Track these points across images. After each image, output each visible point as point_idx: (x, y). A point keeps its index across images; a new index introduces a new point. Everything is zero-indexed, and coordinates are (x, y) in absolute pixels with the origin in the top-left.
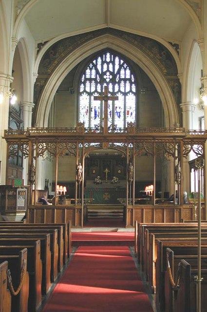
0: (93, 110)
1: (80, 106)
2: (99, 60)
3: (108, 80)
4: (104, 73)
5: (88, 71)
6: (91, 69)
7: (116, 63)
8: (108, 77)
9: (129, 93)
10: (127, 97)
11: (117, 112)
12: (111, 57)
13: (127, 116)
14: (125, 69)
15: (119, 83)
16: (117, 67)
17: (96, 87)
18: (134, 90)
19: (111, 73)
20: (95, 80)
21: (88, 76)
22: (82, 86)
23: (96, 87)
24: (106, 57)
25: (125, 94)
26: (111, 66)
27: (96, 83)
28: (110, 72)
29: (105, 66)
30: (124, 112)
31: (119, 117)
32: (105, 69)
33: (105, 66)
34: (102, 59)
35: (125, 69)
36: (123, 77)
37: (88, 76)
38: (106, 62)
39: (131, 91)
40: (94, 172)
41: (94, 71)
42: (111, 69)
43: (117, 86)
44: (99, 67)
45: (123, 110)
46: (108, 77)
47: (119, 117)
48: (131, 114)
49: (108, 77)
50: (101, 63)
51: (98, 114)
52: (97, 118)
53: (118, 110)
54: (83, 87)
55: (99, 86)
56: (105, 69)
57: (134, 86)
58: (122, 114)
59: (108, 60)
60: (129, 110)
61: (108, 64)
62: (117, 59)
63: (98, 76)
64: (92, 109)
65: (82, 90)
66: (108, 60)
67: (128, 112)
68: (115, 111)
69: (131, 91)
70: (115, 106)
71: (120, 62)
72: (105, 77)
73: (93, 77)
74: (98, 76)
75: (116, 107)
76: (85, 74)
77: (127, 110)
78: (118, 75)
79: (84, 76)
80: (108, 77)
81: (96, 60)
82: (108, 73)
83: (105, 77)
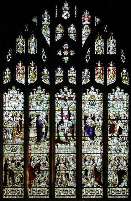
0: (33, 122)
1: (5, 113)
3: (66, 59)
5: (20, 41)
6: (27, 38)
8: (66, 54)
9: (113, 86)
10: (111, 97)
11: (87, 127)
15: (92, 68)
16: (86, 32)
17: (39, 75)
19: (74, 45)
20: (37, 57)
22: (8, 72)
23: (39, 75)
25: (105, 90)
26: (72, 29)
27: (40, 67)
31: (93, 136)
32: (59, 37)
36: (99, 51)
37: (20, 51)
38: (60, 20)
41: (33, 42)
43: (86, 73)
44: (46, 32)
47: (93, 136)
49: (66, 54)
51: (44, 130)
52: (43, 139)
56: (59, 37)
58: (98, 133)
59: (66, 15)
60: (114, 122)
62: (86, 16)
63: (43, 50)
64: (31, 119)
67: (113, 126)
73: (32, 51)
74: (43, 50)
75: (86, 117)
78: (89, 50)
79: (10, 50)
82: (66, 46)
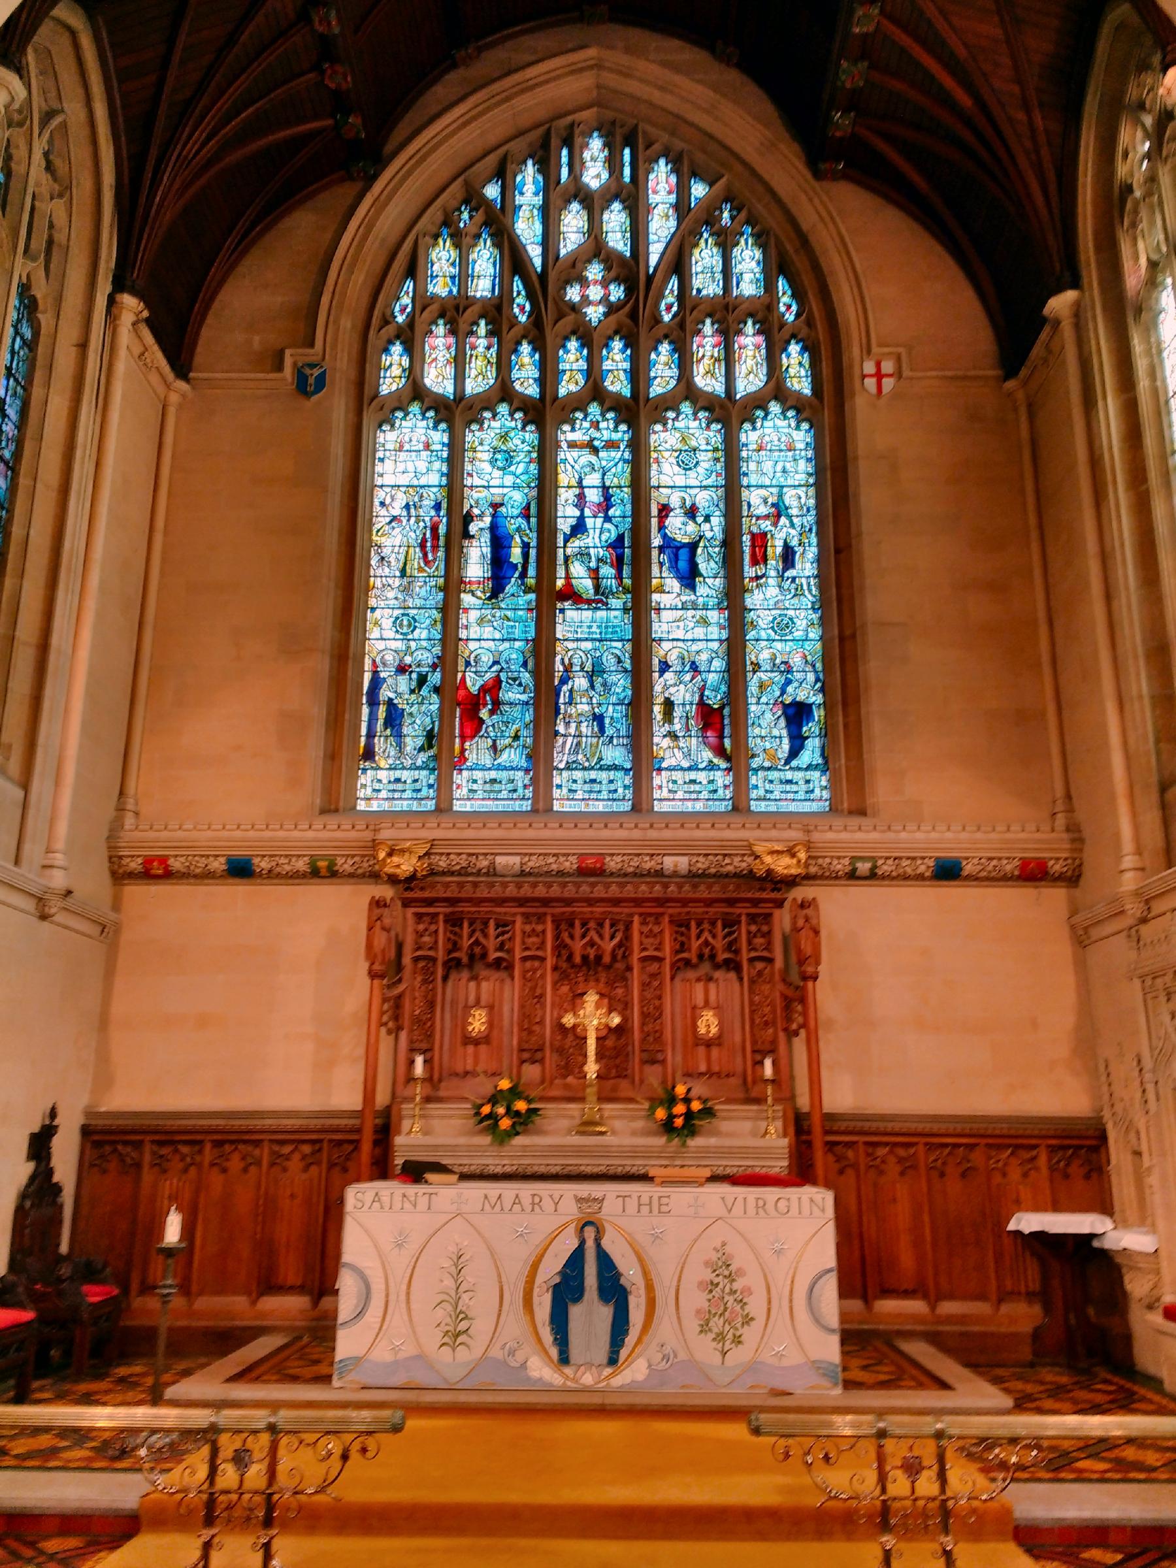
1: (380, 495)
2: (529, 178)
3: (594, 313)
4: (574, 272)
5: (442, 257)
7: (653, 199)
10: (749, 437)
11: (669, 545)
12: (613, 165)
13: (749, 571)
14: (725, 244)
18: (799, 380)
21: (440, 288)
22: (396, 359)
23: (503, 366)
24: (576, 166)
26: (615, 220)
28: (609, 259)
29: (573, 222)
30: (730, 542)
31: (690, 578)
33: (573, 222)
34: (546, 167)
35: (725, 244)
39: (776, 389)
40: (478, 1023)
42: (617, 240)
44: (527, 229)
45: (715, 528)
46: (595, 293)
47: (690, 578)
48: (788, 557)
50: (538, 200)
51: (516, 555)
52: (511, 588)
53: (679, 528)
54: (405, 362)
55: (526, 359)
57: (795, 360)
58: (708, 565)
59: (595, 175)
60: (766, 525)
61: (593, 204)
63: (518, 285)
64: (468, 518)
65: (391, 382)
66: (595, 175)
67: (760, 540)
68: (656, 541)
69: (776, 389)
70: (658, 497)
71: (682, 191)
72: (573, 294)
73: (482, 288)
75: (665, 510)
76: (412, 270)
77: (749, 525)
78: (674, 283)
80: (595, 293)
81: (503, 174)
82: (594, 271)
83: (573, 294)
